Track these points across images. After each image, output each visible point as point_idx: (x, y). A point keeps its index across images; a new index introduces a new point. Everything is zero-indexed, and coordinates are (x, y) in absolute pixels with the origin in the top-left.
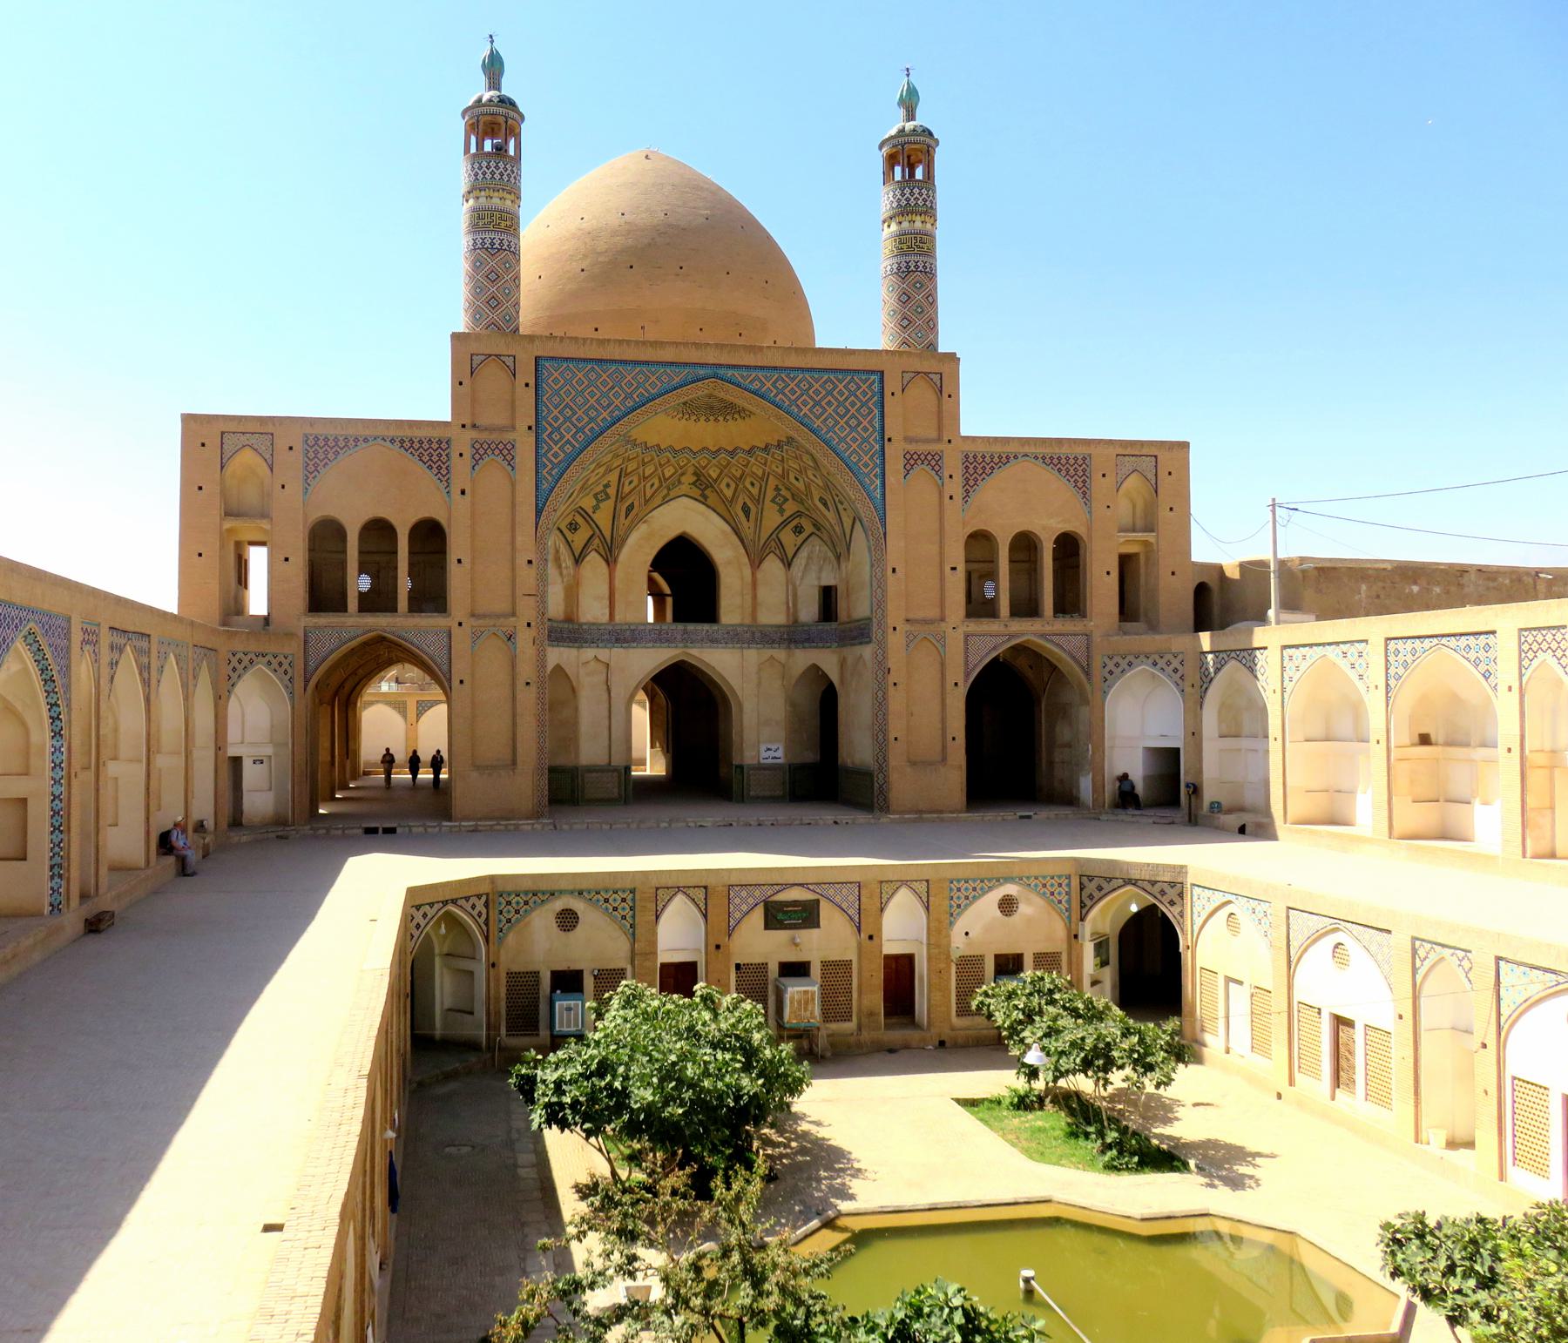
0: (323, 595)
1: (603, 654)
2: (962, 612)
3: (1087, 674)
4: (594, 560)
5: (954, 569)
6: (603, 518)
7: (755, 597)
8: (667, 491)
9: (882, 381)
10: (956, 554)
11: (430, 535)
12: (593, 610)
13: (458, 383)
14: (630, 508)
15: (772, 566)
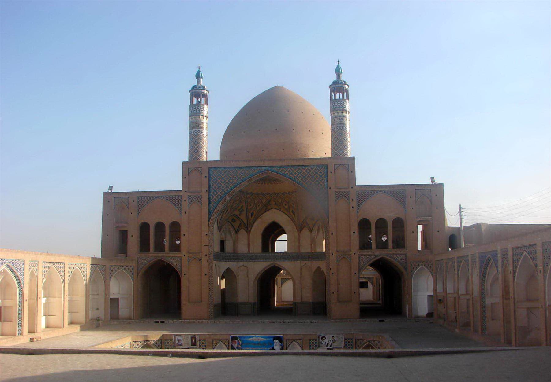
0: (144, 246)
1: (245, 264)
2: (357, 247)
3: (406, 269)
4: (243, 232)
5: (354, 232)
6: (243, 217)
7: (299, 243)
8: (266, 208)
9: (327, 168)
10: (355, 227)
11: (175, 227)
12: (242, 248)
13: (184, 178)
14: (252, 214)
15: (306, 232)
